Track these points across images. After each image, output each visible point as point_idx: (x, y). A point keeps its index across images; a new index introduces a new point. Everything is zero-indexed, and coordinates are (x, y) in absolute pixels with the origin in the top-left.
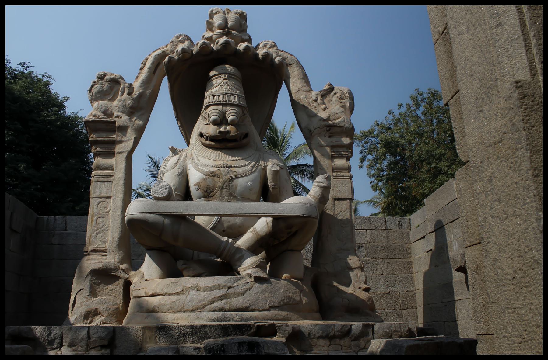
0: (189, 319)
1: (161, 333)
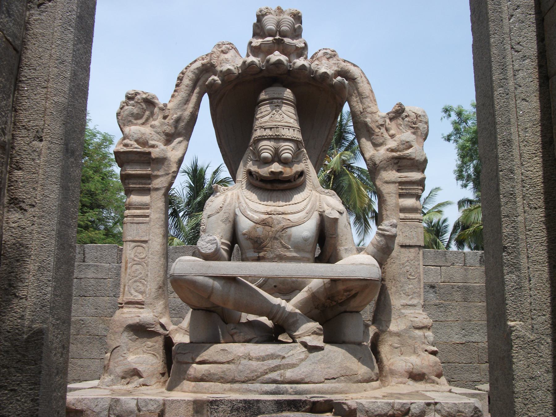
1: (212, 407)
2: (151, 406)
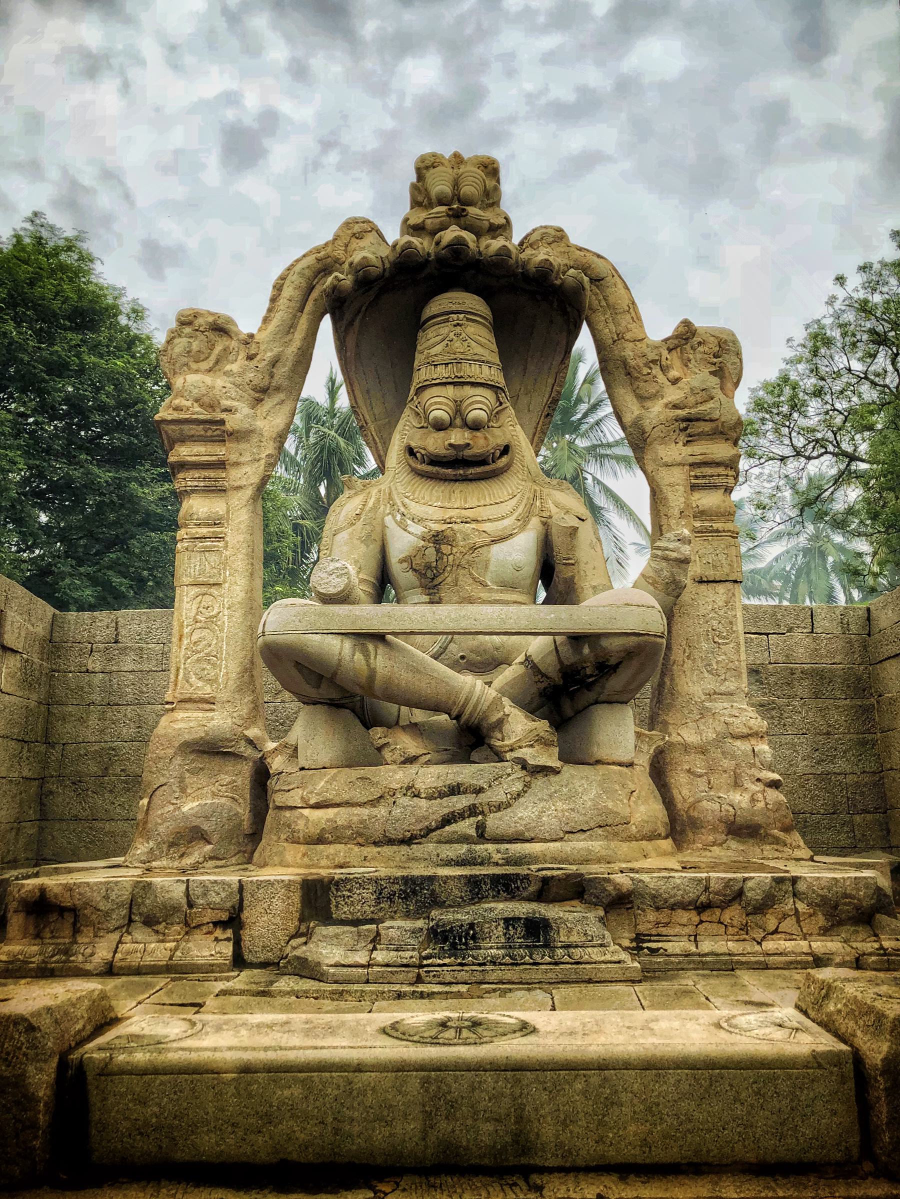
0: (398, 859)
2: (214, 894)
